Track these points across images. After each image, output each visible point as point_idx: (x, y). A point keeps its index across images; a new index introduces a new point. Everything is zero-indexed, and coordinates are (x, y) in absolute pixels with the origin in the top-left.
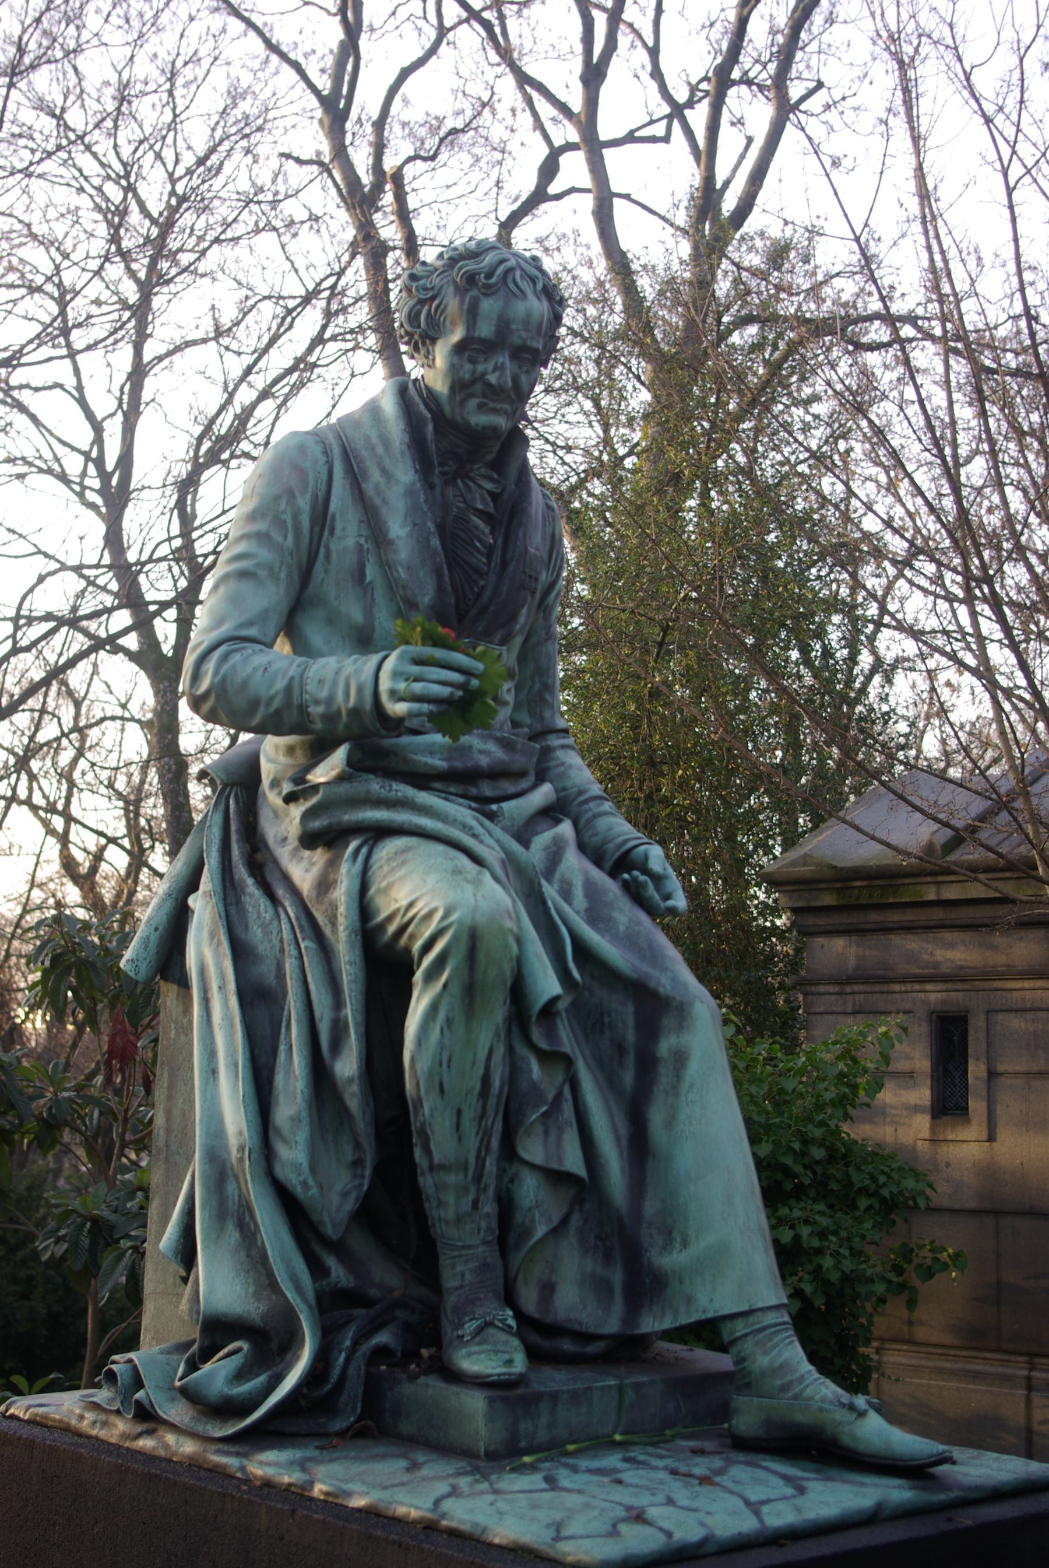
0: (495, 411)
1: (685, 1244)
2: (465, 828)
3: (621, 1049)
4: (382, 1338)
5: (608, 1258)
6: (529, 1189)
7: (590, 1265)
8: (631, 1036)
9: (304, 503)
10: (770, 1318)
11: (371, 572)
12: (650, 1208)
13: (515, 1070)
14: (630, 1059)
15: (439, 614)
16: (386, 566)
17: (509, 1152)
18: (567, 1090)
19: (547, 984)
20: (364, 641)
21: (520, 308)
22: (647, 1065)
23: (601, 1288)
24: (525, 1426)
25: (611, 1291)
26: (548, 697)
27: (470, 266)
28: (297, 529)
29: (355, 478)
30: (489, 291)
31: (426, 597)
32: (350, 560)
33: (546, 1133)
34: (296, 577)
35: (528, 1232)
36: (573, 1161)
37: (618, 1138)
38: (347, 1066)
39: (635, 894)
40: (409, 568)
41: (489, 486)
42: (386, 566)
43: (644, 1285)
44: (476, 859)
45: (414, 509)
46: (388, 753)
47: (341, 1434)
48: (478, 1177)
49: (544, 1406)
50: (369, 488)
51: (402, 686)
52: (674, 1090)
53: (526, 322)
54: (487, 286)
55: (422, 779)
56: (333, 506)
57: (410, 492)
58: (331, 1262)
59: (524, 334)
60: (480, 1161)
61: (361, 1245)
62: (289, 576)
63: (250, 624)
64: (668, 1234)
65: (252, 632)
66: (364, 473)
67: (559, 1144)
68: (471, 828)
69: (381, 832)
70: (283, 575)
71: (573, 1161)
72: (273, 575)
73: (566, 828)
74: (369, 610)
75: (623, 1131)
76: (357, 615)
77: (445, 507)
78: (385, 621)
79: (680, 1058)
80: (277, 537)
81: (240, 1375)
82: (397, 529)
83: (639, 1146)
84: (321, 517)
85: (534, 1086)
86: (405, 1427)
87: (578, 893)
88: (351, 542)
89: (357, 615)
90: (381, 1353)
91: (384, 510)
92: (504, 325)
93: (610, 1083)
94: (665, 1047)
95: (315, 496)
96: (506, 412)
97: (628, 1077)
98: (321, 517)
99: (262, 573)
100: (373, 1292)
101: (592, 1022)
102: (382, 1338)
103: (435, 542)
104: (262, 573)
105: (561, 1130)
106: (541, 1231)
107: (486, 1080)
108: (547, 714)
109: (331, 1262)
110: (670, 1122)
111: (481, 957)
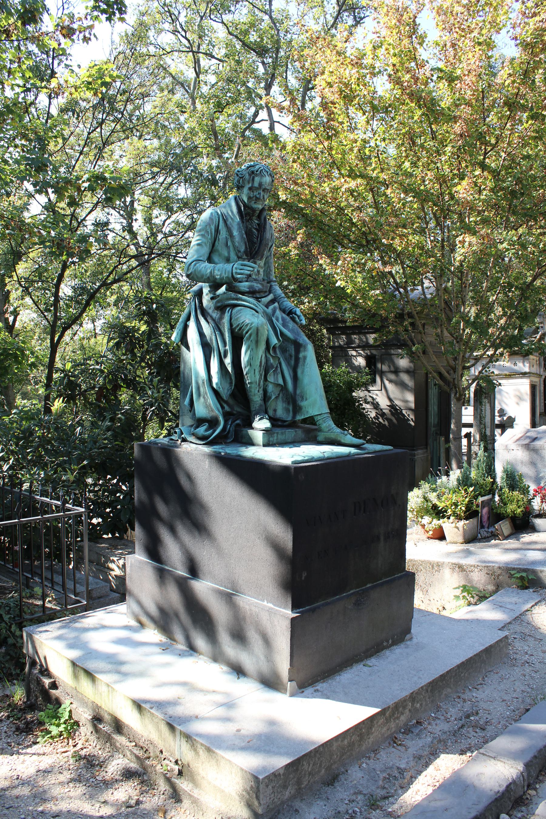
1: (306, 400)
2: (254, 304)
3: (291, 356)
4: (238, 422)
5: (289, 404)
6: (270, 388)
8: (293, 353)
9: (213, 227)
10: (325, 415)
11: (229, 243)
12: (298, 392)
13: (267, 360)
14: (293, 358)
15: (246, 252)
16: (233, 242)
17: (266, 379)
19: (274, 341)
20: (228, 260)
22: (297, 360)
23: (287, 410)
24: (271, 439)
25: (289, 411)
27: (252, 169)
28: (211, 233)
29: (225, 221)
30: (257, 175)
31: (243, 249)
32: (224, 241)
35: (270, 398)
38: (228, 361)
39: (293, 319)
41: (256, 222)
42: (233, 242)
43: (297, 409)
44: (257, 312)
45: (239, 228)
46: (235, 287)
47: (230, 442)
48: (259, 385)
49: (275, 435)
50: (228, 223)
51: (239, 271)
52: (304, 365)
55: (243, 293)
56: (220, 227)
57: (238, 224)
58: (225, 406)
60: (260, 381)
61: (231, 402)
64: (302, 398)
65: (201, 259)
66: (227, 219)
67: (277, 378)
69: (235, 306)
71: (281, 382)
73: (276, 304)
74: (229, 253)
75: (292, 375)
76: (226, 254)
77: (247, 227)
78: (233, 256)
79: (305, 358)
80: (206, 235)
81: (206, 430)
82: (235, 233)
83: (295, 378)
84: (217, 231)
85: (272, 364)
86: (244, 441)
87: (280, 319)
88: (224, 236)
89: (226, 254)
90: (238, 425)
91: (232, 229)
93: (288, 364)
94: (301, 355)
97: (293, 362)
98: (217, 231)
99: (203, 244)
100: (235, 412)
101: (284, 350)
102: (238, 422)
103: (245, 236)
104: (203, 244)
106: (273, 397)
107: (261, 362)
109: (225, 406)
110: (303, 372)
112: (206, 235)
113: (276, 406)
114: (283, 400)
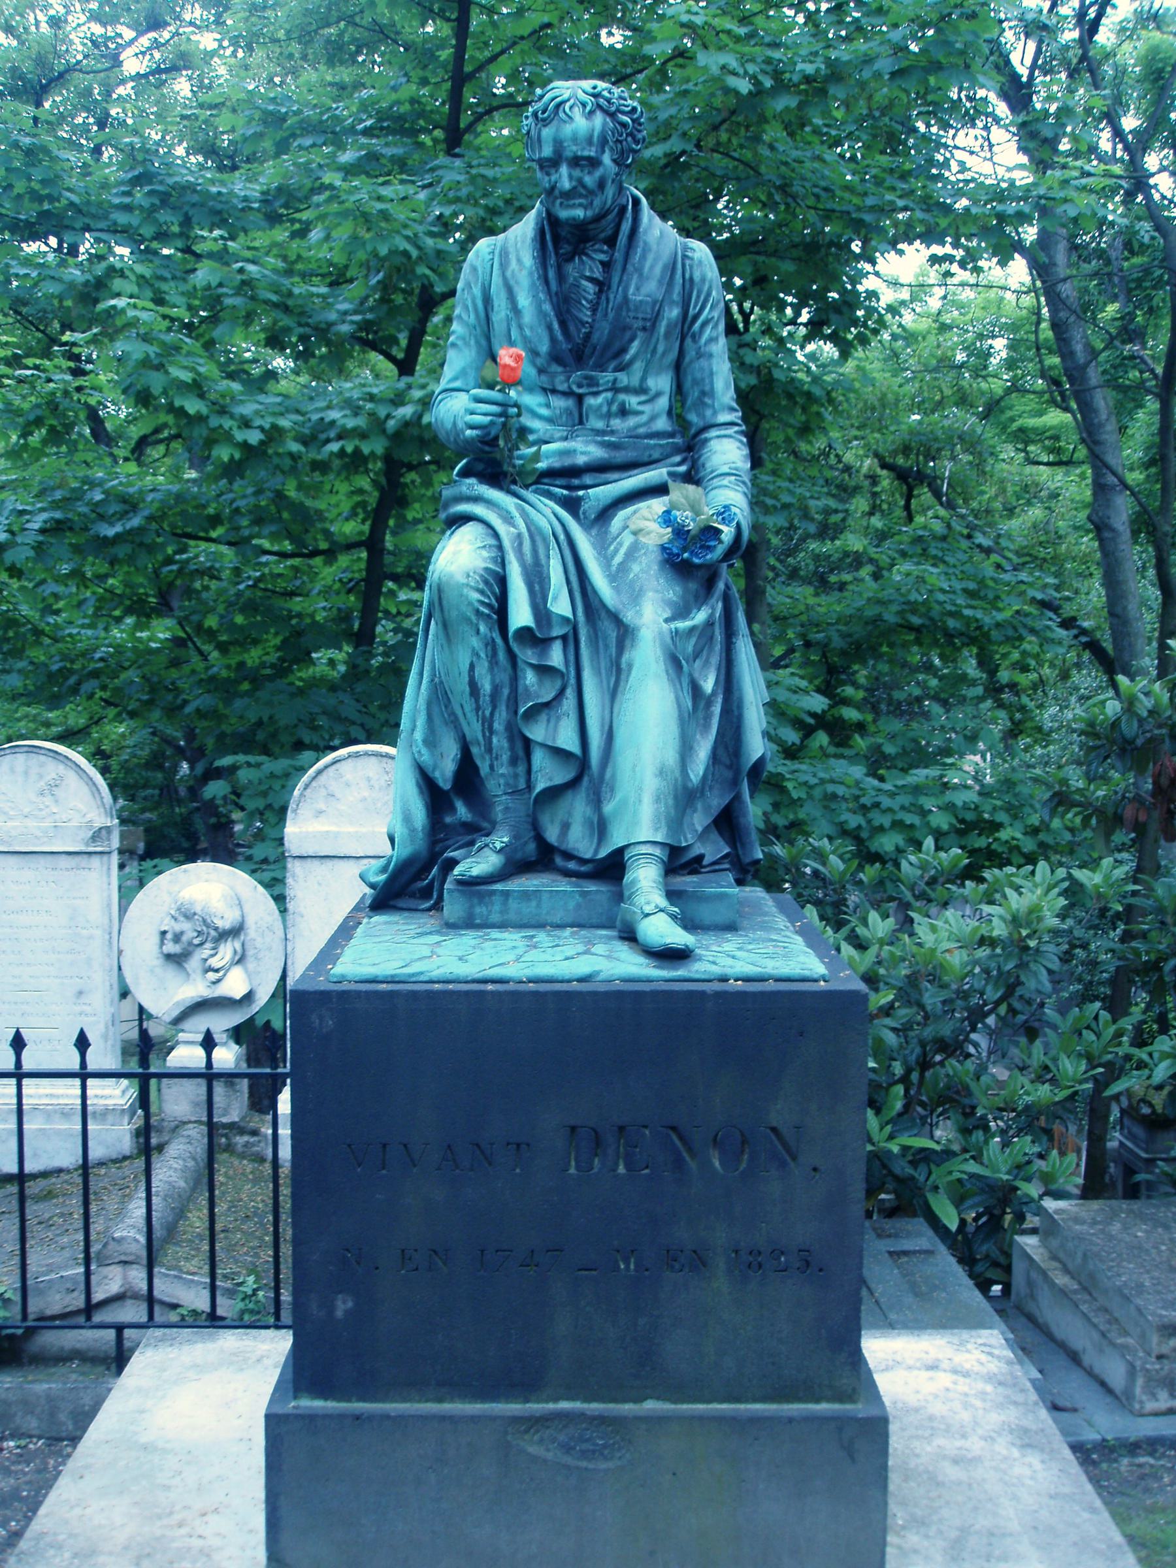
0: (573, 206)
7: (589, 811)
9: (477, 291)
11: (514, 334)
12: (608, 775)
16: (520, 327)
18: (570, 693)
21: (568, 130)
22: (619, 670)
26: (708, 401)
29: (504, 266)
30: (546, 122)
31: (544, 348)
32: (505, 325)
33: (548, 721)
34: (484, 342)
36: (567, 739)
37: (603, 726)
40: (531, 328)
42: (520, 327)
43: (601, 828)
45: (533, 284)
48: (489, 749)
49: (497, 899)
50: (508, 274)
53: (575, 139)
54: (543, 120)
59: (574, 148)
62: (477, 342)
63: (455, 379)
68: (508, 512)
70: (472, 342)
72: (467, 344)
79: (630, 666)
84: (487, 300)
88: (503, 314)
91: (516, 289)
92: (558, 144)
94: (624, 660)
95: (483, 285)
96: (580, 205)
103: (547, 307)
105: (558, 719)
108: (709, 413)
111: (445, 603)
112: (465, 316)
113: (570, 814)
114: (588, 795)
